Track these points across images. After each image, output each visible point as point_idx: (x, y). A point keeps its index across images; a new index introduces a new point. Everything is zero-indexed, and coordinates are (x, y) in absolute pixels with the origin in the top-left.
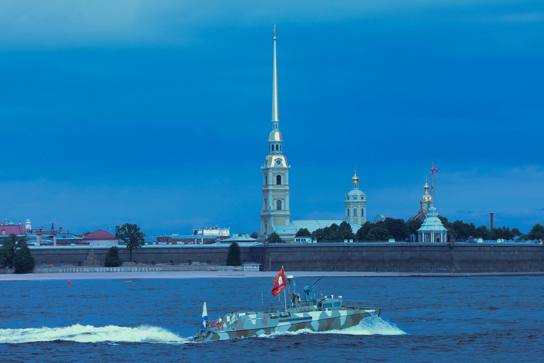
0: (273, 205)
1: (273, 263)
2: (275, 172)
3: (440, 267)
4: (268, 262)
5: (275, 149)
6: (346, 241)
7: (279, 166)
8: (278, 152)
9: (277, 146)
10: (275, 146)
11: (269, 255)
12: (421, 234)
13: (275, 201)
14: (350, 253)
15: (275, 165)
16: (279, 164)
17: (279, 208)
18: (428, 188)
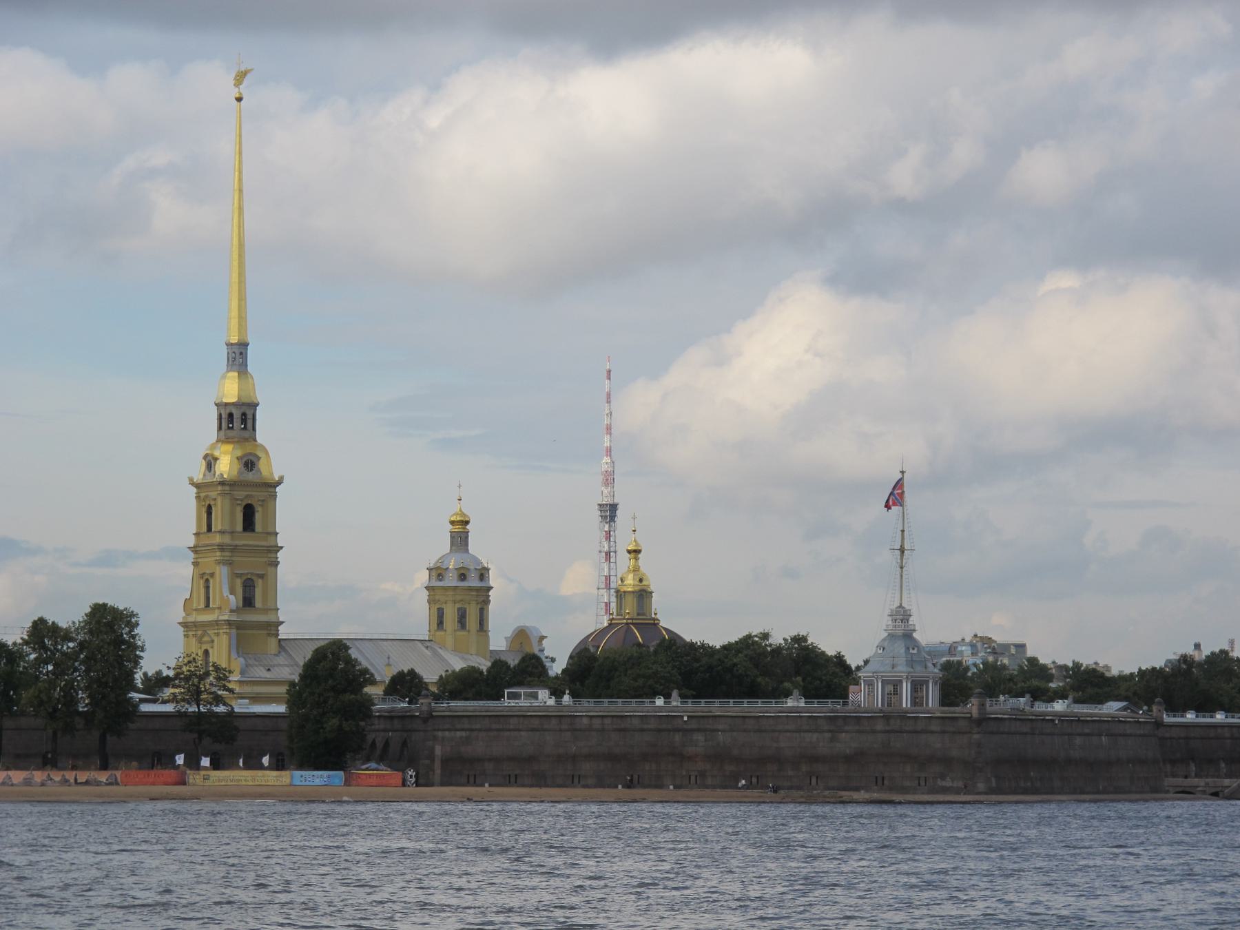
0: (232, 592)
1: (446, 761)
2: (240, 494)
3: (943, 777)
4: (431, 757)
6: (660, 702)
7: (250, 476)
9: (244, 414)
10: (237, 415)
11: (435, 738)
12: (870, 684)
13: (239, 582)
14: (678, 737)
15: (240, 473)
18: (637, 552)
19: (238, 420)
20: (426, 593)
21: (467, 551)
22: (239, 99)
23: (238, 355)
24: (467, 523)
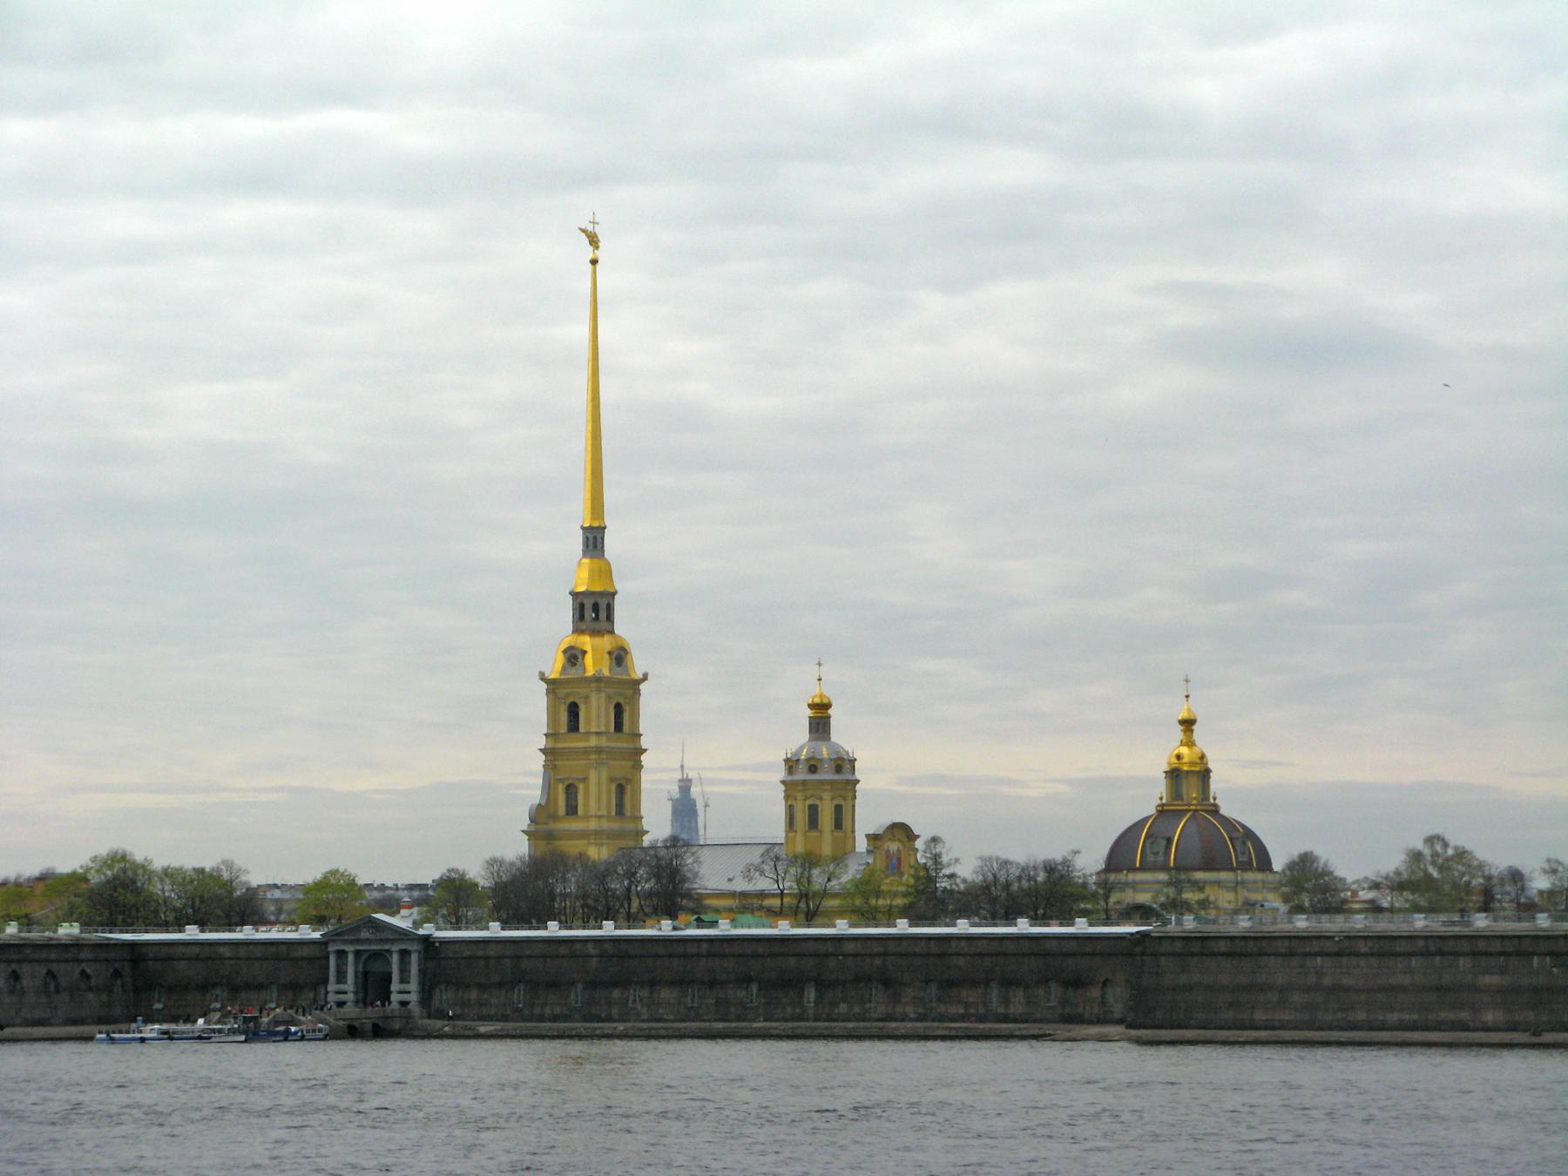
2: (562, 692)
5: (603, 615)
7: (573, 673)
8: (583, 626)
10: (588, 604)
13: (561, 788)
15: (564, 669)
16: (574, 665)
17: (572, 810)
19: (594, 610)
20: (783, 788)
21: (829, 739)
22: (594, 262)
23: (594, 540)
24: (827, 706)
